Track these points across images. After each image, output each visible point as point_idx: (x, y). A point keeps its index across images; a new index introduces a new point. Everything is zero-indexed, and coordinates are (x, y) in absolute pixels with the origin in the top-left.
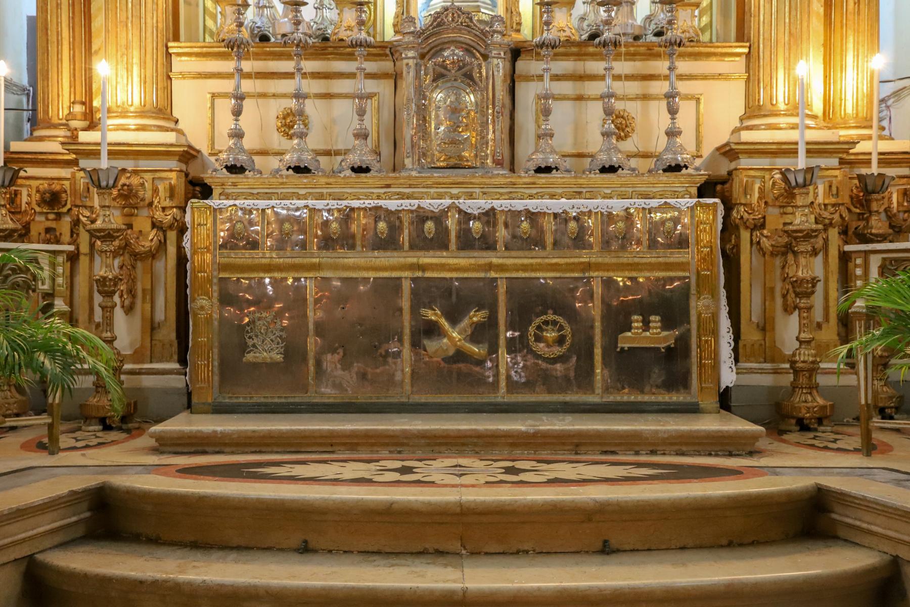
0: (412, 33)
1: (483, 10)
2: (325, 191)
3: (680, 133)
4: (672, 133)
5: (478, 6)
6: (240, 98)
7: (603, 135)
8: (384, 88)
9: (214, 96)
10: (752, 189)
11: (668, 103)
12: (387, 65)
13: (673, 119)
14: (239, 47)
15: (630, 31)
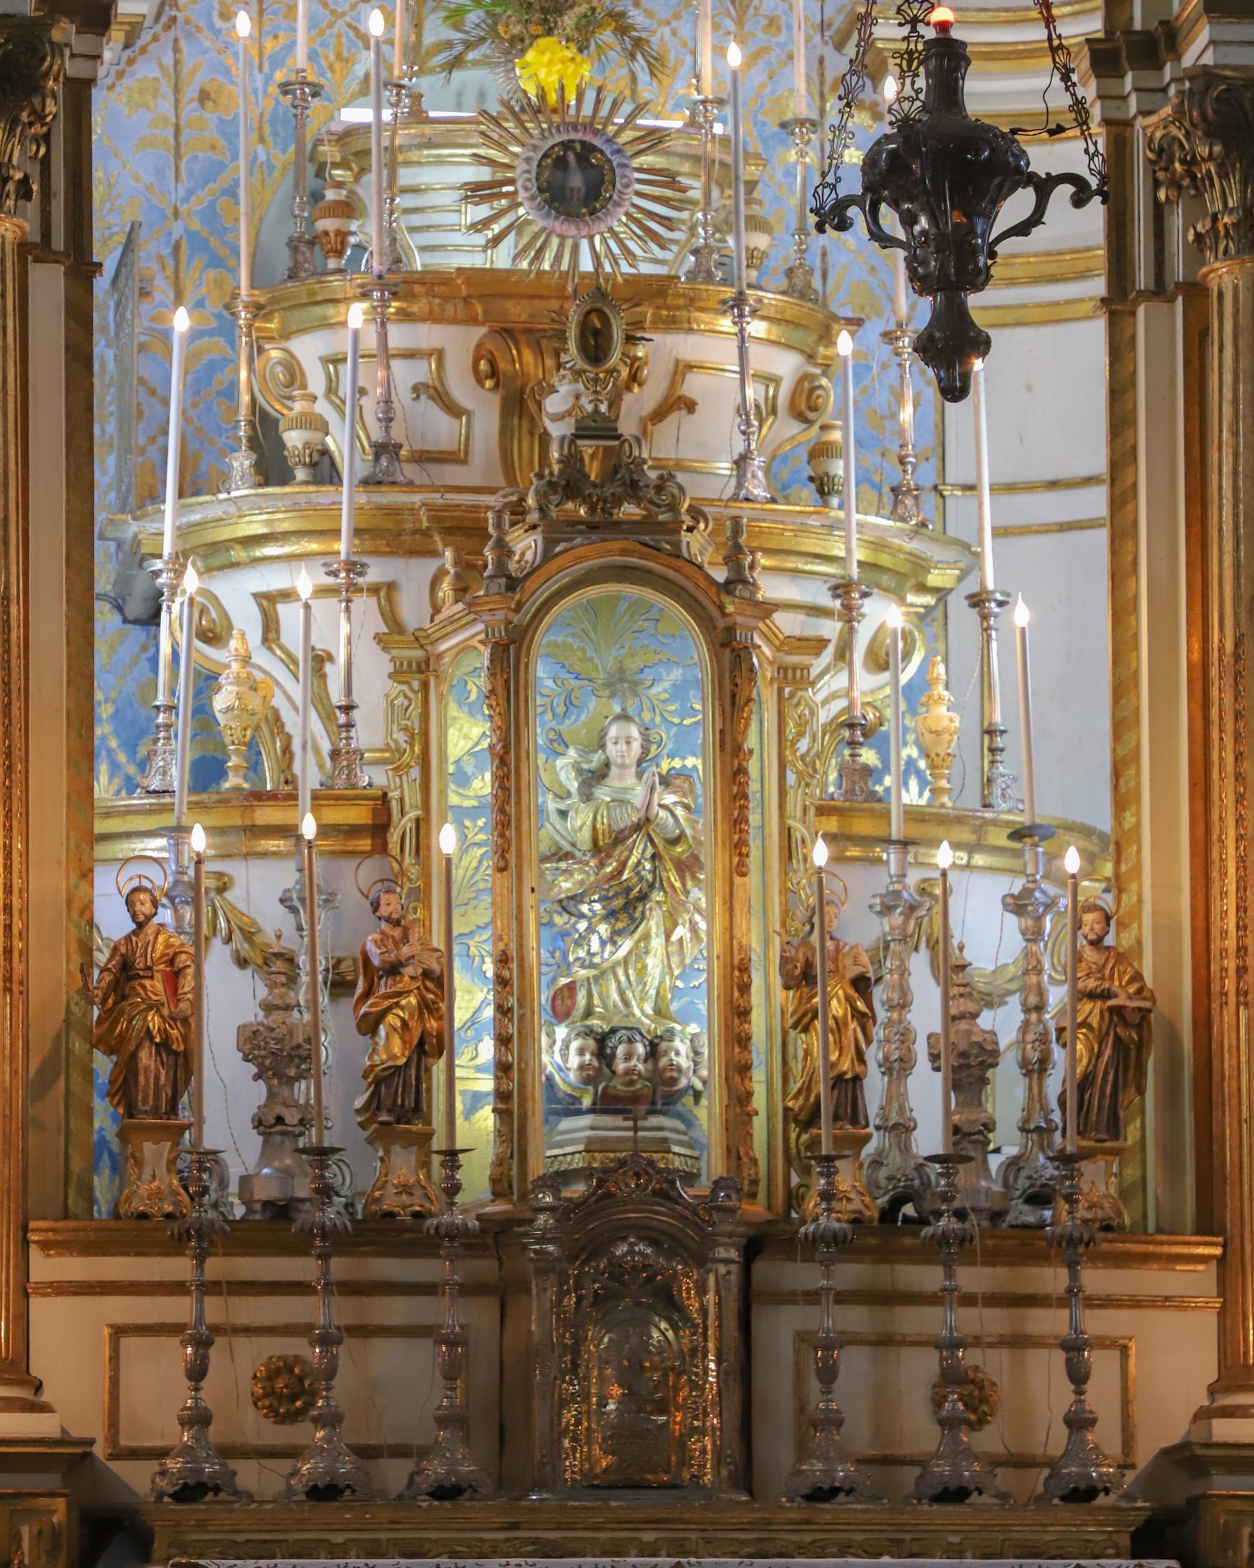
0: (550, 1209)
1: (676, 1149)
2: (383, 1536)
3: (1092, 1422)
4: (1078, 1422)
5: (665, 1140)
6: (202, 1344)
7: (942, 1423)
8: (479, 1317)
9: (119, 1331)
10: (1237, 1540)
11: (1069, 1362)
12: (485, 1268)
13: (1079, 1392)
14: (200, 1238)
15: (983, 1204)
